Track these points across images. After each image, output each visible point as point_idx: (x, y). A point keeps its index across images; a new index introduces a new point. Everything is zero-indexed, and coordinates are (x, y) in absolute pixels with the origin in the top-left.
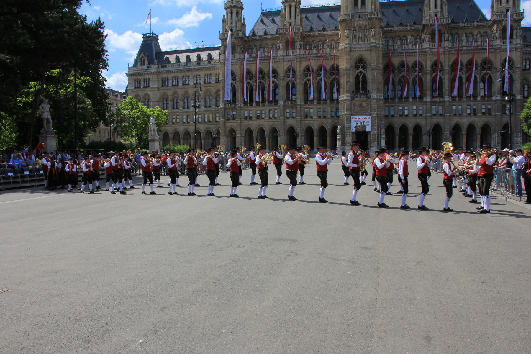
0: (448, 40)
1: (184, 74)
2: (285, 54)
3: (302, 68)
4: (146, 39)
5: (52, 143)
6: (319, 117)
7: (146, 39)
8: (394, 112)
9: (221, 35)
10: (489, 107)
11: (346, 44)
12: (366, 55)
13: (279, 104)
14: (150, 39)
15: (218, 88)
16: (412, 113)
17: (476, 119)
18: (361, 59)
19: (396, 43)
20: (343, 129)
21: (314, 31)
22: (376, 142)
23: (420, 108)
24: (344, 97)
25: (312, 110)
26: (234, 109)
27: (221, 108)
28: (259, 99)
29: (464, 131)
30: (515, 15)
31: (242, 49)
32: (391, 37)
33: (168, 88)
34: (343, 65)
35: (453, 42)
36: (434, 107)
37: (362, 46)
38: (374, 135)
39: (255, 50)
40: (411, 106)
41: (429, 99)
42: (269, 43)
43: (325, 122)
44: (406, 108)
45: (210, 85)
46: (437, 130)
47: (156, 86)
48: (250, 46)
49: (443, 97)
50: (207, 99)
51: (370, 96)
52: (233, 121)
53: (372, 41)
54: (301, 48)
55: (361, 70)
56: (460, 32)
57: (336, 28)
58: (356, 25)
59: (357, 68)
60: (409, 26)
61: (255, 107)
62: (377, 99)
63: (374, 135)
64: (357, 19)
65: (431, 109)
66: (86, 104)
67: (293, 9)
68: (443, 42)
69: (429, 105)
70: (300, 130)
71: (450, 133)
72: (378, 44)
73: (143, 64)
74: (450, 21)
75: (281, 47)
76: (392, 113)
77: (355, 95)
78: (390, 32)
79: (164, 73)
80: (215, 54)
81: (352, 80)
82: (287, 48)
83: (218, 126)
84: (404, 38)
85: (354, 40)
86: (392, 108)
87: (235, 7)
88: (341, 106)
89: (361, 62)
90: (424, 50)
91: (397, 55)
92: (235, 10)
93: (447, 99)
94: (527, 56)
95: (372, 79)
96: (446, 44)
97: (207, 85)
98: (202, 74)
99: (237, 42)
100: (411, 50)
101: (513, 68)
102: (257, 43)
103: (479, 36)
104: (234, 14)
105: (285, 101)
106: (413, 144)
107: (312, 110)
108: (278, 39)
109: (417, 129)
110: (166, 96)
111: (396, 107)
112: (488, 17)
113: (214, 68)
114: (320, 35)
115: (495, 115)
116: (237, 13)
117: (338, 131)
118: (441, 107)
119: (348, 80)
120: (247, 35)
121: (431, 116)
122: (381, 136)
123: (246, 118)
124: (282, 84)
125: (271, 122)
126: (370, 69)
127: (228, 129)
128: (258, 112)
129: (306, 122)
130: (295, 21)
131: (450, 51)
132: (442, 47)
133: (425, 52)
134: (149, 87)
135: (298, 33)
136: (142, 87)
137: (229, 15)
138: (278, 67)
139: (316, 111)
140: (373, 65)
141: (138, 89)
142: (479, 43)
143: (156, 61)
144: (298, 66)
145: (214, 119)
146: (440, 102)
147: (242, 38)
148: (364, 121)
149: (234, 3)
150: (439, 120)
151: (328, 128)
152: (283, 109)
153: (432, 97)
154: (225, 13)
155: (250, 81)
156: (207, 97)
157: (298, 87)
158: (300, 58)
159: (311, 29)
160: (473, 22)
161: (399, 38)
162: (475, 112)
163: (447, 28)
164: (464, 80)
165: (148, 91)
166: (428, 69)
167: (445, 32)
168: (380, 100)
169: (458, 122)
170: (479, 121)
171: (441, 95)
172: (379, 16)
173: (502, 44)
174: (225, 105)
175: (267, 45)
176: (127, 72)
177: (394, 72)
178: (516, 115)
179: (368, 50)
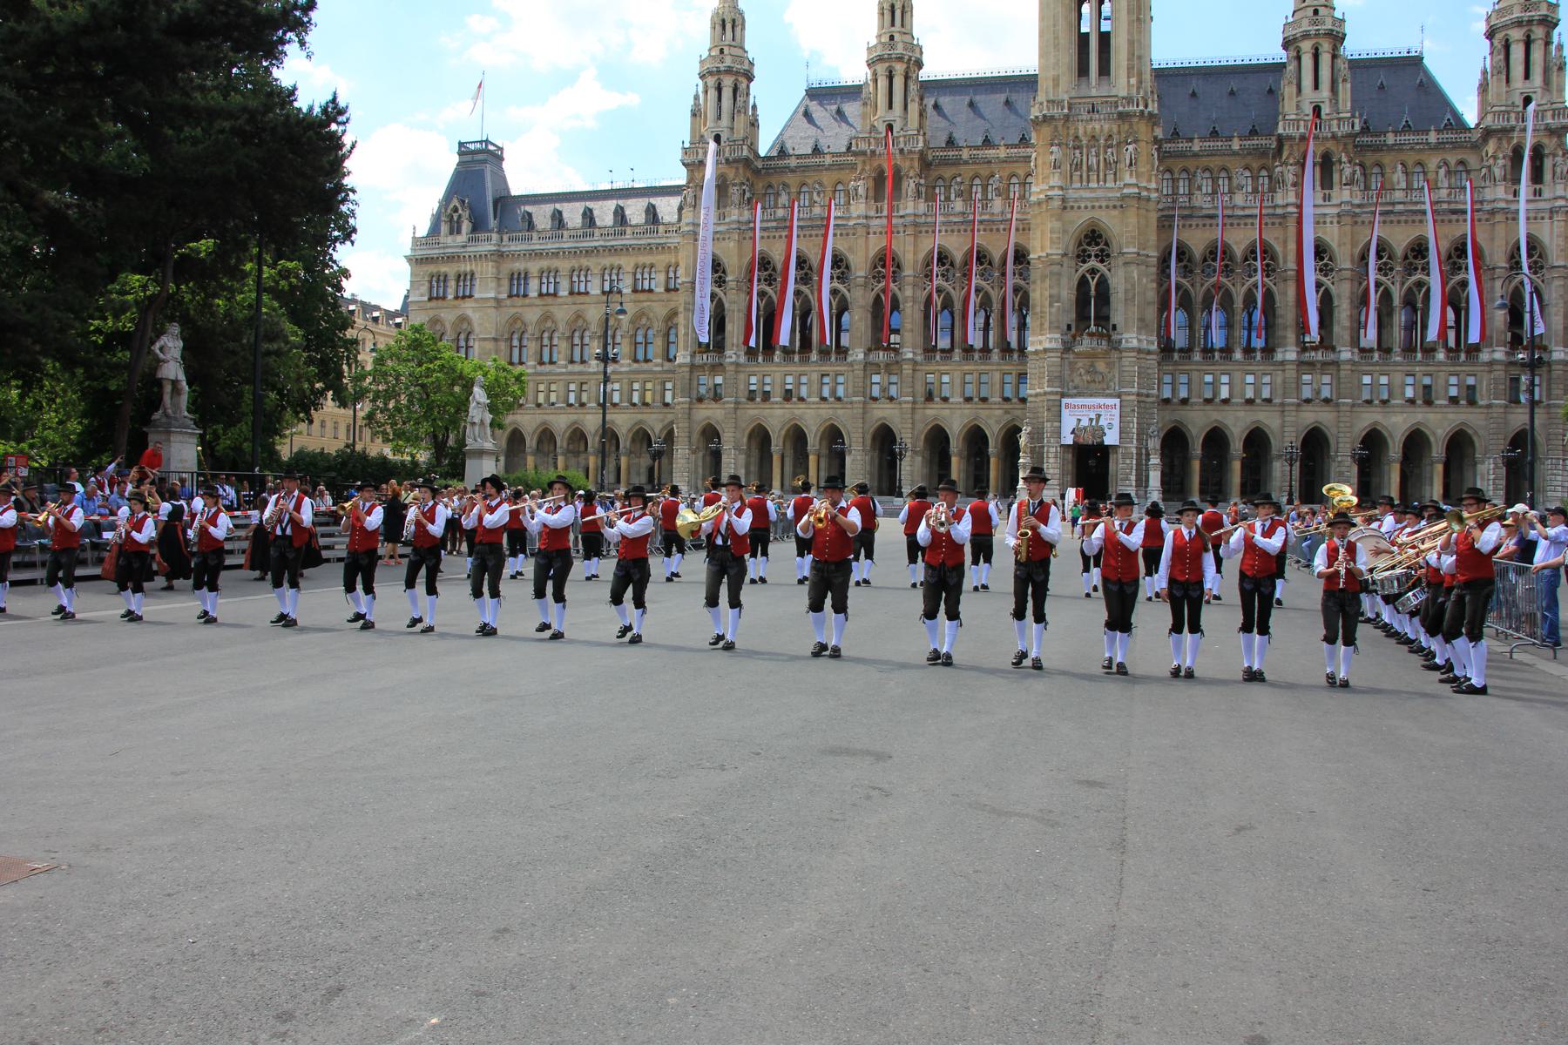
1: (574, 263)
2: (872, 213)
4: (468, 158)
5: (183, 453)
6: (968, 400)
7: (468, 158)
8: (1190, 391)
9: (686, 151)
10: (1471, 381)
11: (1052, 188)
13: (850, 359)
14: (480, 157)
15: (672, 305)
16: (1242, 395)
17: (1431, 416)
18: (1093, 231)
19: (1200, 188)
20: (1037, 436)
21: (960, 148)
22: (1133, 478)
23: (1267, 379)
24: (1042, 340)
25: (946, 379)
26: (717, 368)
27: (680, 366)
28: (792, 340)
29: (1395, 450)
30: (1549, 114)
31: (748, 195)
32: (1185, 170)
33: (527, 301)
34: (1042, 249)
35: (1367, 188)
36: (1306, 378)
37: (1099, 194)
38: (1126, 455)
39: (784, 199)
40: (1237, 375)
41: (1292, 355)
42: (828, 178)
43: (983, 414)
44: (1225, 379)
45: (650, 296)
46: (1314, 446)
47: (492, 295)
48: (770, 186)
49: (1333, 349)
50: (640, 339)
51: (1120, 342)
52: (714, 405)
53: (1128, 179)
55: (1093, 263)
56: (1387, 159)
57: (1024, 141)
58: (1081, 132)
59: (1082, 257)
60: (1236, 140)
61: (778, 365)
62: (1139, 351)
63: (1126, 455)
64: (1085, 116)
65: (1299, 384)
66: (287, 342)
68: (1336, 188)
69: (1291, 373)
70: (910, 436)
71: (1353, 457)
72: (1148, 189)
73: (455, 229)
74: (1357, 128)
75: (861, 191)
76: (1183, 394)
77: (1074, 337)
78: (1182, 155)
79: (515, 256)
80: (667, 208)
81: (1068, 293)
83: (670, 417)
84: (1223, 174)
86: (1183, 379)
87: (729, 71)
88: (1032, 367)
89: (1093, 241)
90: (1279, 211)
91: (1201, 222)
92: (728, 82)
93: (1346, 354)
95: (1126, 291)
96: (1345, 195)
97: (642, 297)
98: (627, 262)
99: (731, 174)
100: (1243, 208)
101: (1542, 267)
102: (792, 180)
103: (1442, 171)
104: (727, 93)
105: (870, 350)
106: (1243, 485)
107: (946, 379)
108: (853, 167)
109: (1257, 441)
110: (519, 324)
111: (1195, 375)
112: (1471, 117)
113: (662, 248)
114: (974, 160)
115: (1489, 406)
116: (735, 90)
117: (1023, 440)
118: (1326, 379)
119: (1055, 291)
120: (762, 152)
121: (1298, 405)
122: (1148, 459)
123: (751, 396)
124: (860, 299)
125: (826, 412)
126: (1121, 261)
127: (698, 428)
128: (789, 379)
129: (928, 412)
131: (1356, 215)
132: (1334, 201)
133: (1284, 216)
134: (471, 296)
135: (910, 152)
136: (450, 297)
137: (712, 93)
138: (850, 249)
139: (958, 381)
141: (440, 303)
142: (1444, 193)
143: (493, 223)
144: (910, 248)
145: (658, 398)
146: (1324, 364)
147: (747, 162)
148: (1097, 414)
149: (728, 61)
150: (1322, 416)
151: (994, 432)
152: (861, 373)
153: (1303, 348)
154: (701, 89)
156: (641, 332)
157: (908, 311)
158: (916, 225)
159: (950, 142)
160: (1427, 132)
161: (1207, 175)
162: (1428, 396)
163: (1350, 147)
164: (1397, 301)
165: (468, 308)
167: (1344, 159)
168: (1149, 352)
169: (1376, 423)
170: (1439, 424)
171: (1326, 343)
173: (1511, 197)
174: (693, 355)
175: (821, 184)
176: (409, 253)
177: (1191, 272)
178: (1549, 406)
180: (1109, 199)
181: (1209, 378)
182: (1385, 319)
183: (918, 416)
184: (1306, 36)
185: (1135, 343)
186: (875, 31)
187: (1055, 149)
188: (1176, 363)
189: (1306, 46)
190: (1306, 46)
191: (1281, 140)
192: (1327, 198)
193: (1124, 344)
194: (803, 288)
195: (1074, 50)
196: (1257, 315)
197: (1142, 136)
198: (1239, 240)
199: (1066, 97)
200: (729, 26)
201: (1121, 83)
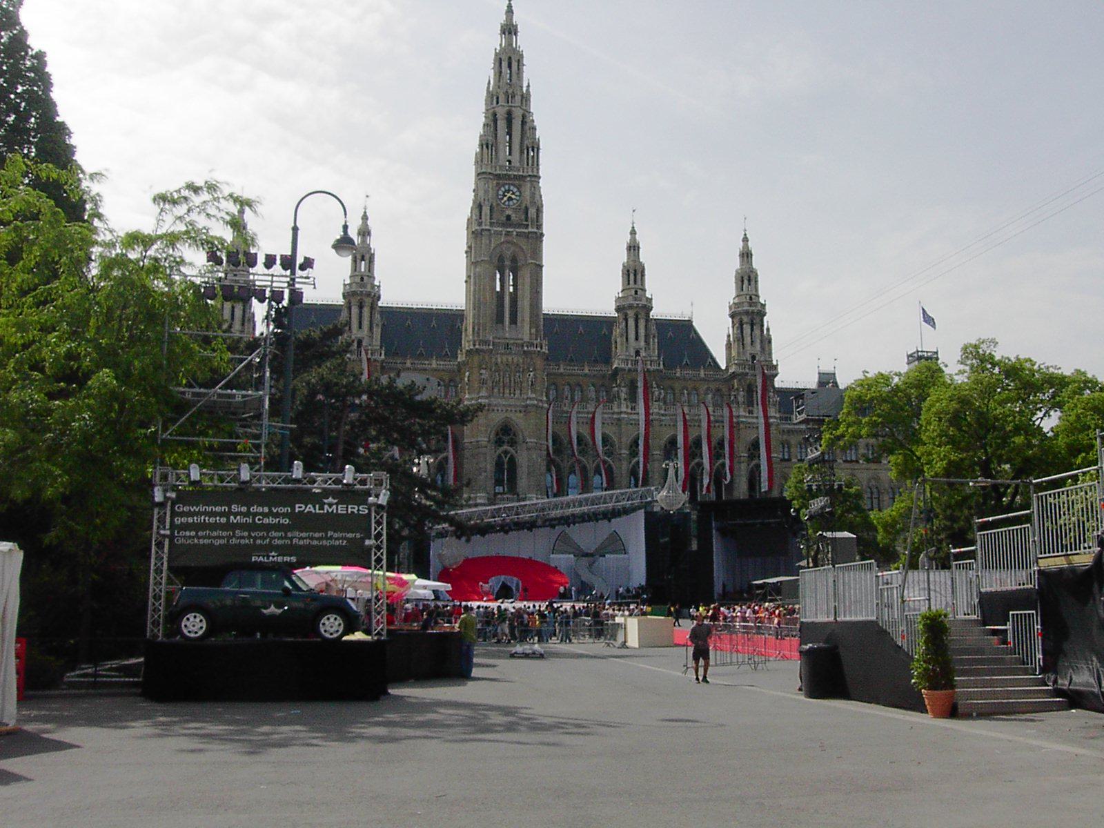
12: (518, 419)
18: (506, 426)
37: (512, 402)
58: (499, 360)
59: (499, 443)
67: (366, 311)
74: (662, 366)
81: (490, 466)
85: (496, 390)
89: (505, 434)
90: (615, 416)
94: (785, 437)
103: (710, 396)
130: (371, 337)
133: (619, 420)
135: (375, 360)
140: (531, 440)
166: (625, 452)
167: (655, 386)
172: (544, 350)
179: (520, 412)
180: (515, 406)
184: (631, 307)
186: (349, 273)
187: (483, 371)
189: (631, 313)
190: (631, 313)
191: (616, 371)
199: (491, 338)
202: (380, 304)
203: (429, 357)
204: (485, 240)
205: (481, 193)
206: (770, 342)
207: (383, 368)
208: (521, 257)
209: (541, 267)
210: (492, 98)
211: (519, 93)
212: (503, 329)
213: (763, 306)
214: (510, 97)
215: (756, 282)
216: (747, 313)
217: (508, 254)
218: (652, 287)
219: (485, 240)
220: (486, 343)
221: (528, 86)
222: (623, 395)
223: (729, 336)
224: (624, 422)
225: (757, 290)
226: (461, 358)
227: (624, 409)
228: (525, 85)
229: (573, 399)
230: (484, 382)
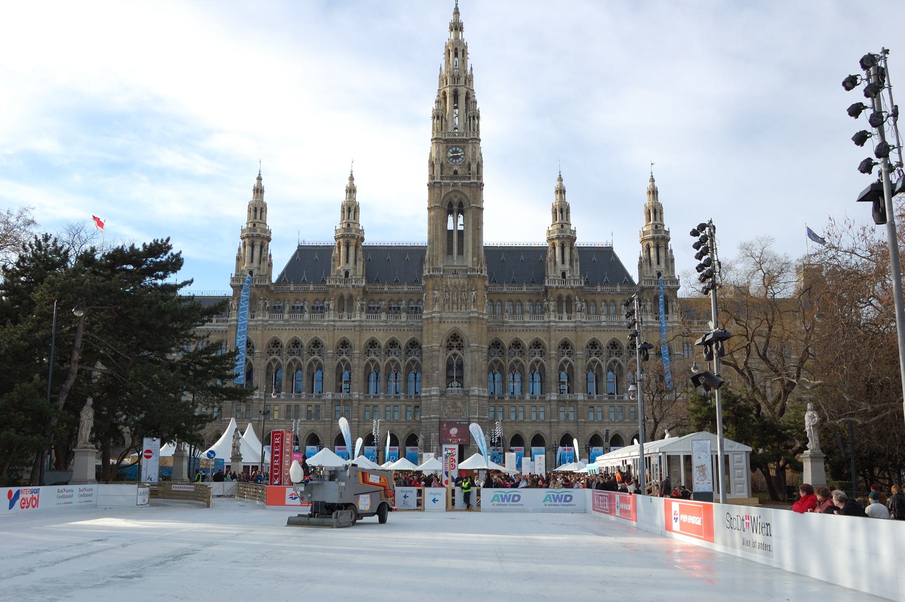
0: (581, 311)
2: (337, 319)
3: (363, 343)
9: (233, 279)
11: (435, 312)
12: (464, 329)
23: (542, 409)
31: (268, 305)
36: (562, 409)
37: (458, 315)
40: (527, 407)
41: (554, 397)
44: (521, 409)
51: (469, 391)
53: (473, 309)
54: (362, 310)
55: (455, 351)
59: (450, 347)
61: (283, 400)
62: (479, 396)
67: (352, 250)
69: (554, 406)
75: (331, 307)
81: (442, 366)
82: (340, 309)
85: (446, 307)
86: (501, 409)
87: (258, 236)
89: (455, 340)
92: (258, 243)
93: (581, 397)
95: (472, 366)
111: (506, 407)
116: (262, 247)
118: (571, 409)
124: (330, 364)
132: (573, 320)
133: (549, 327)
137: (248, 248)
138: (324, 337)
149: (259, 232)
155: (277, 357)
157: (356, 372)
181: (513, 409)
182: (599, 378)
183: (361, 429)
185: (477, 392)
187: (436, 292)
188: (496, 401)
192: (569, 318)
193: (471, 393)
194: (298, 358)
195: (445, 242)
196: (537, 377)
197: (479, 287)
198: (527, 340)
200: (259, 212)
201: (469, 260)
202: (363, 244)
203: (402, 284)
204: (437, 191)
205: (434, 155)
206: (673, 260)
207: (365, 293)
208: (465, 202)
209: (481, 209)
210: (442, 79)
211: (463, 75)
212: (453, 258)
213: (667, 232)
214: (456, 78)
215: (661, 213)
216: (653, 239)
217: (456, 200)
218: (576, 221)
219: (437, 191)
220: (438, 270)
221: (471, 69)
222: (552, 308)
223: (641, 258)
224: (552, 329)
225: (661, 219)
226: (424, 283)
227: (552, 318)
228: (469, 69)
229: (514, 313)
230: (436, 300)
